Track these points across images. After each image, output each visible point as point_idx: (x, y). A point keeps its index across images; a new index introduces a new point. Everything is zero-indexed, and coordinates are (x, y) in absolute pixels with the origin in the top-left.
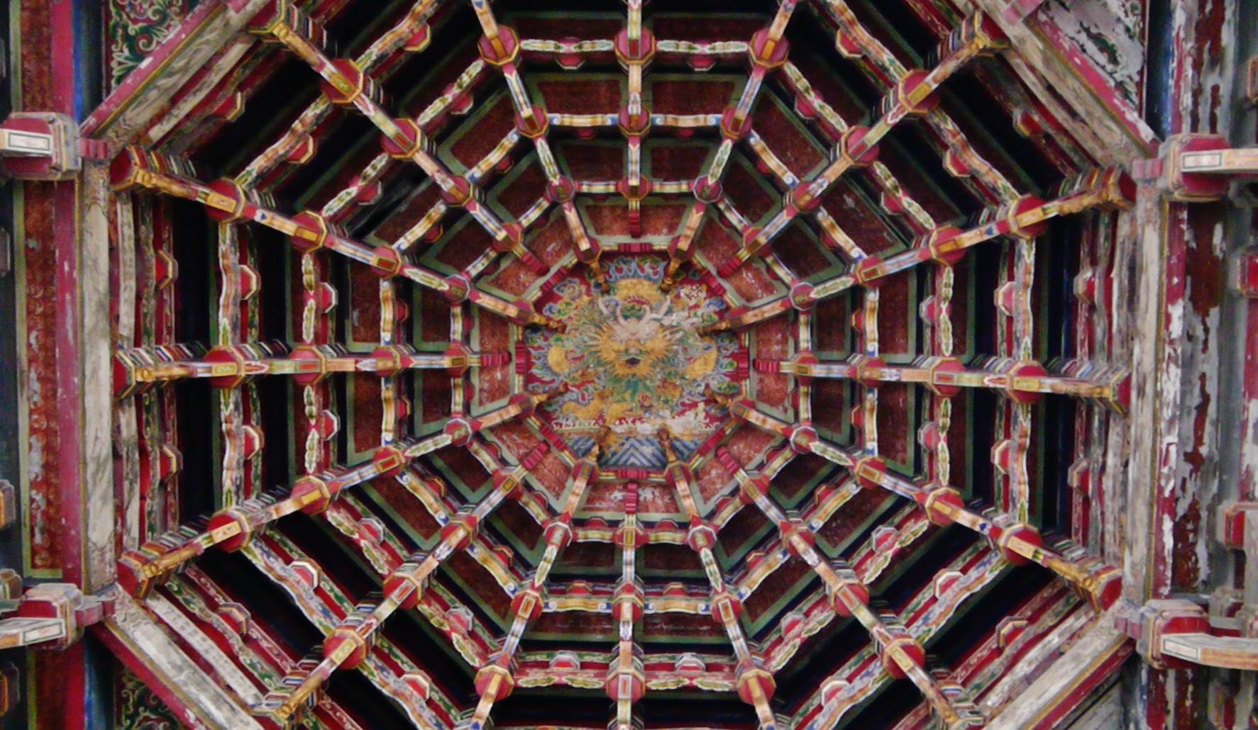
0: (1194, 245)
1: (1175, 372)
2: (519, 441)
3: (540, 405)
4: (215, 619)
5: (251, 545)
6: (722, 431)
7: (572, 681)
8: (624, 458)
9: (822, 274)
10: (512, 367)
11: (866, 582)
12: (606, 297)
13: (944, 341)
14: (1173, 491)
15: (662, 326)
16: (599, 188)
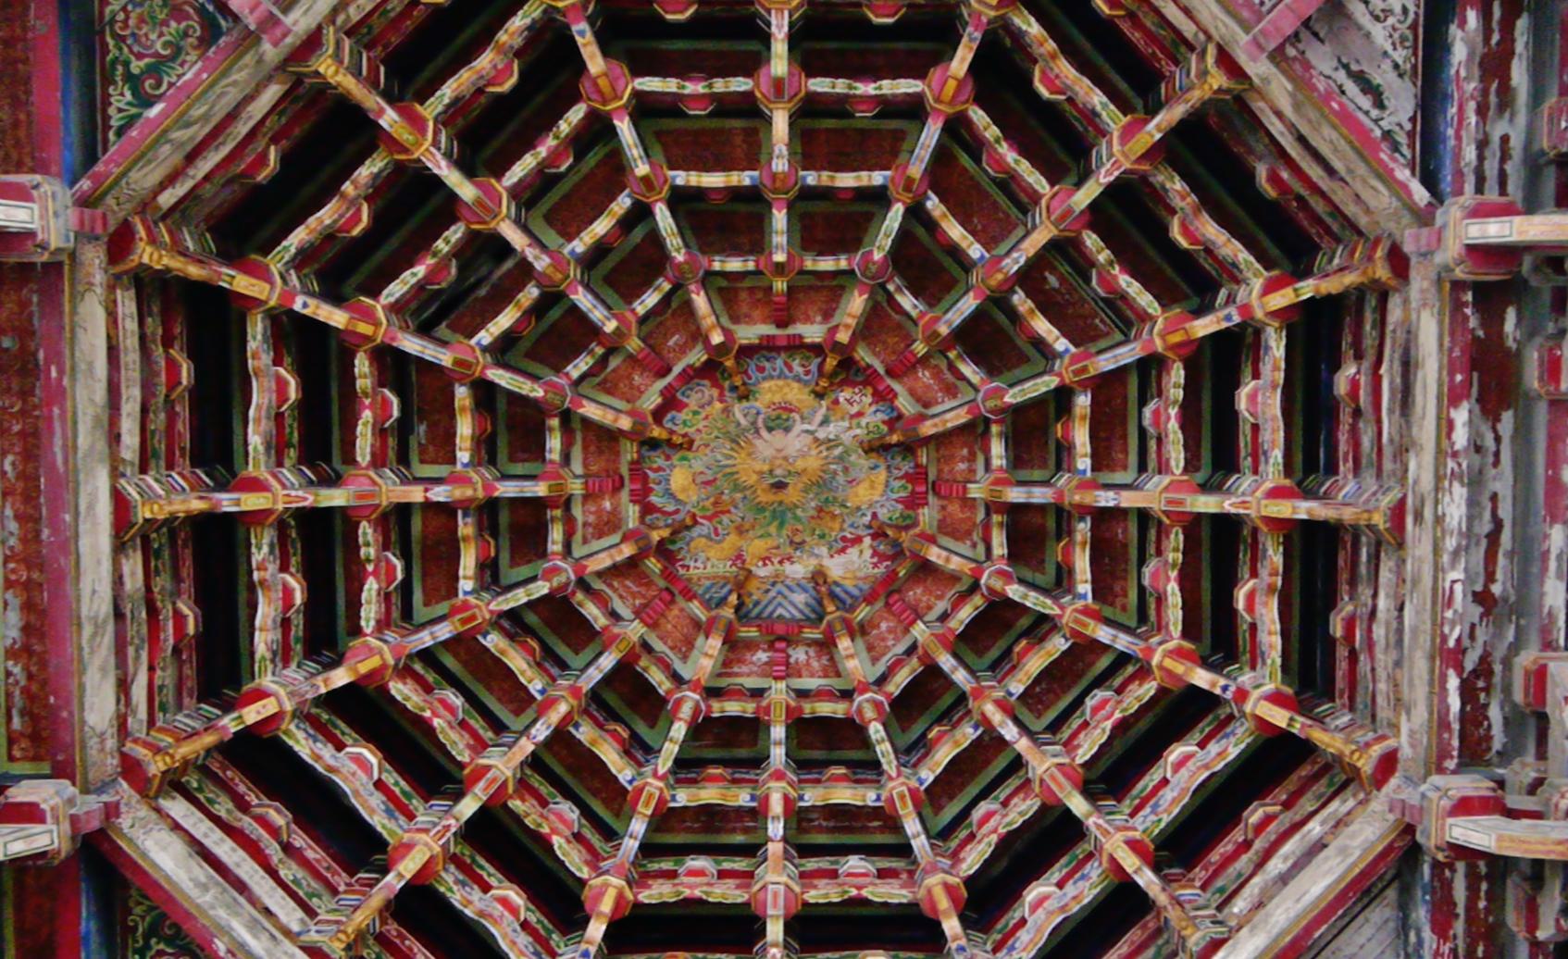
0: (1481, 333)
1: (1460, 492)
3: (662, 542)
4: (247, 823)
5: (292, 727)
6: (895, 572)
7: (707, 893)
8: (770, 608)
9: (1019, 373)
10: (625, 495)
11: (1079, 760)
12: (745, 404)
13: (1173, 455)
14: (1458, 640)
15: (816, 440)
16: (734, 265)
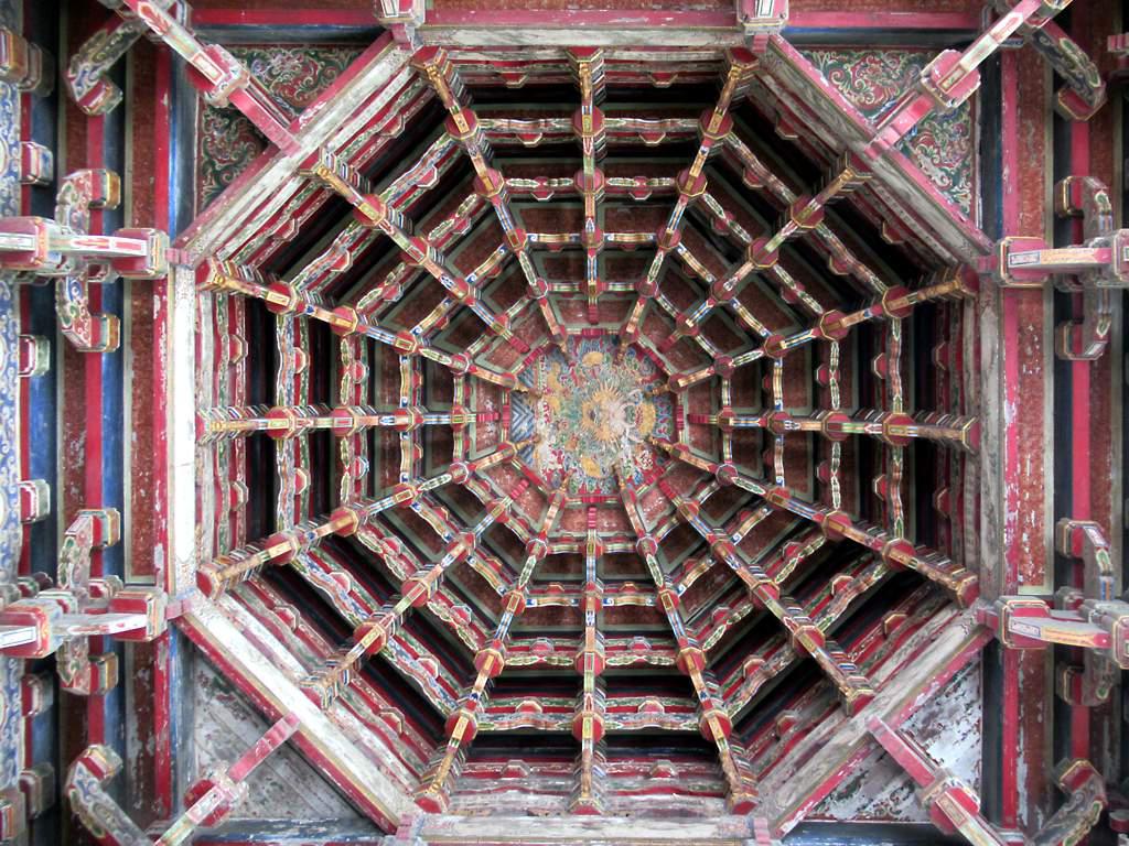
2: (530, 331)
4: (393, 113)
6: (541, 484)
10: (586, 325)
11: (429, 604)
